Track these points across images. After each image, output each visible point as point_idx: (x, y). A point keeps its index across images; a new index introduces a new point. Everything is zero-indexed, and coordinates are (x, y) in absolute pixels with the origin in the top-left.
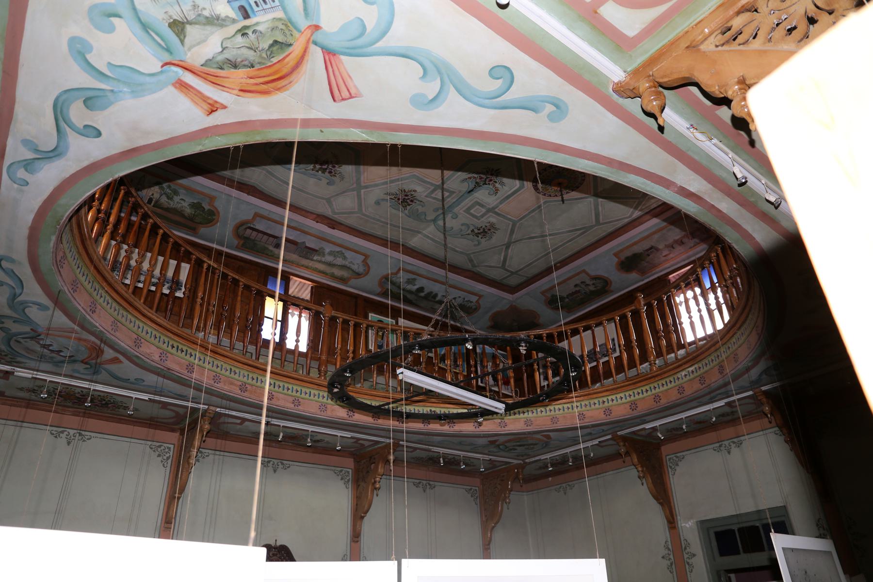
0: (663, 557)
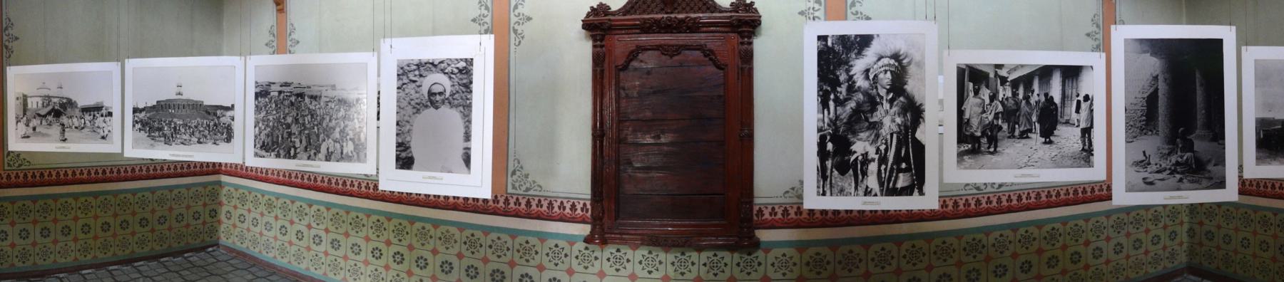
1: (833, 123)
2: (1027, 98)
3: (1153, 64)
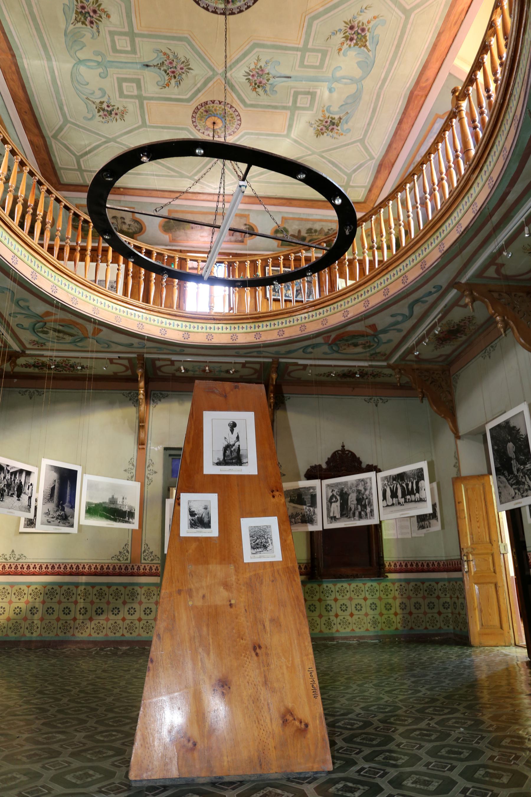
0: (125, 471)
2: (14, 480)
3: (54, 476)
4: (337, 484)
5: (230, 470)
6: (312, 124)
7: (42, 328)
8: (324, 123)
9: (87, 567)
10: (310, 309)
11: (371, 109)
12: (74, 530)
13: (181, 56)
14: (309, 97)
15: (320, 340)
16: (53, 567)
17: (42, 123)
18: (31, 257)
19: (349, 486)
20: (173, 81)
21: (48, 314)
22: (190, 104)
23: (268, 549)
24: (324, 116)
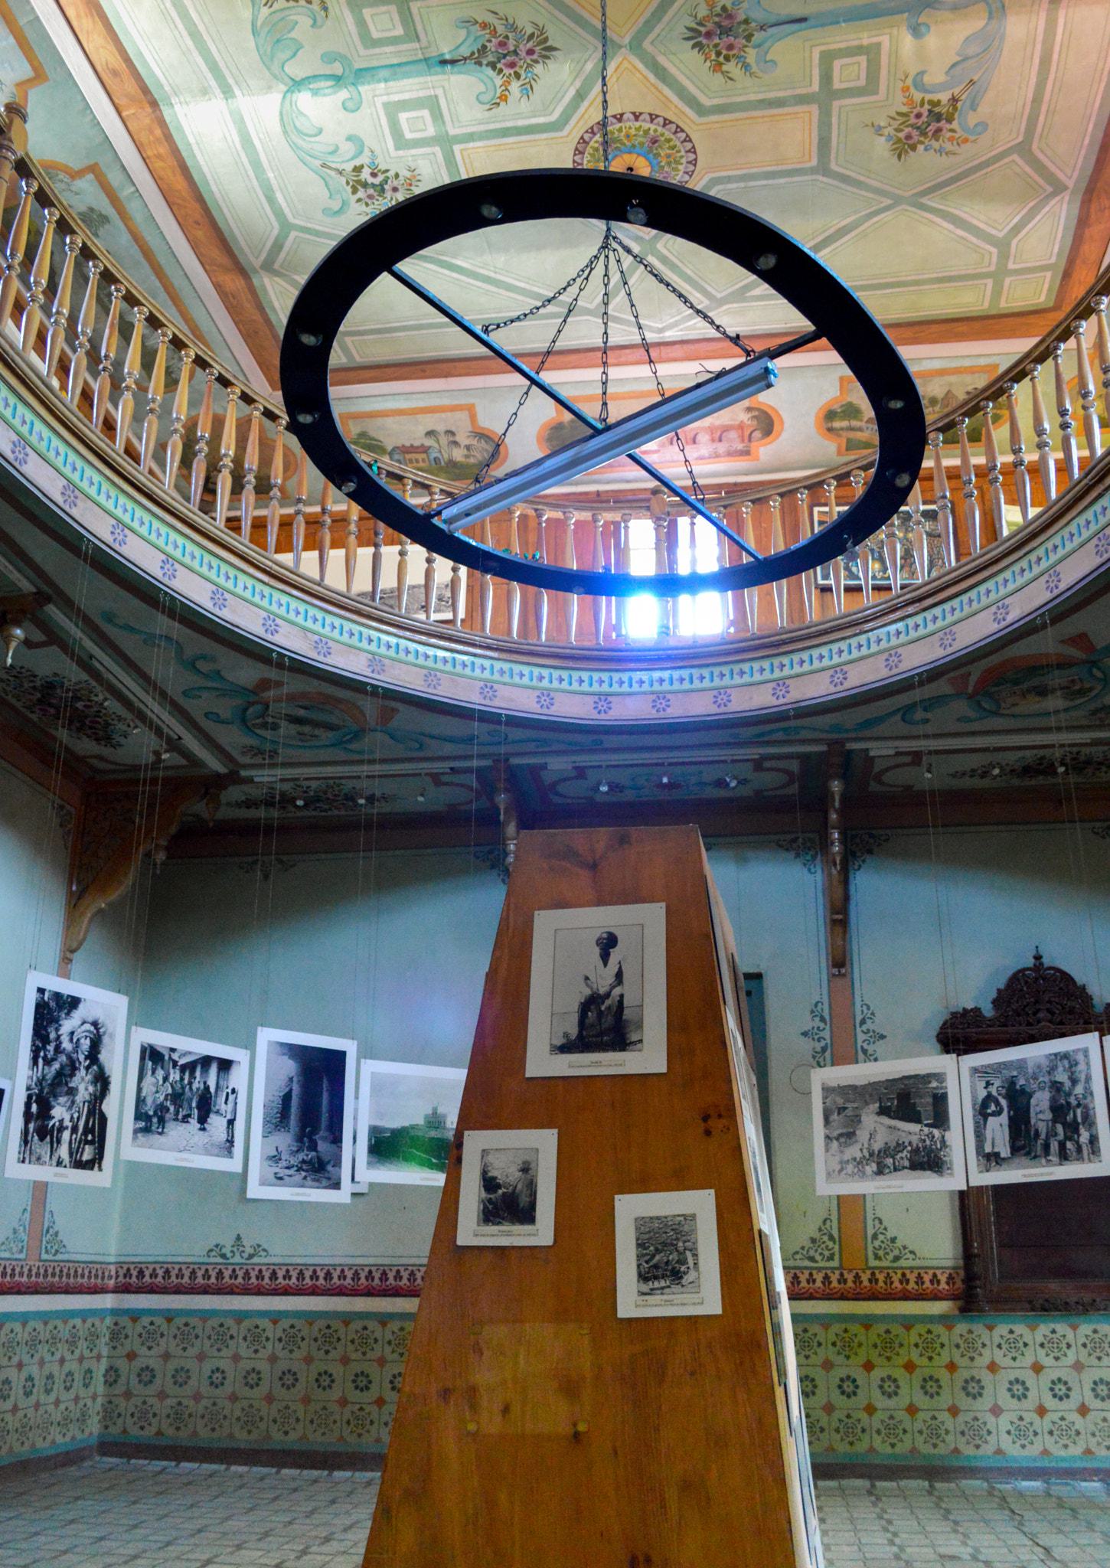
1: (40, 1082)
2: (190, 1083)
3: (289, 1067)
4: (999, 1067)
5: (598, 1064)
6: (880, 128)
7: (262, 716)
8: (913, 120)
9: (405, 1275)
10: (910, 610)
11: (1036, 61)
12: (342, 1197)
13: (525, 21)
14: (863, 59)
15: (942, 687)
16: (328, 1276)
17: (235, 239)
18: (207, 557)
19: (1030, 1071)
20: (515, 86)
21: (264, 684)
22: (565, 133)
23: (684, 1281)
24: (910, 101)
